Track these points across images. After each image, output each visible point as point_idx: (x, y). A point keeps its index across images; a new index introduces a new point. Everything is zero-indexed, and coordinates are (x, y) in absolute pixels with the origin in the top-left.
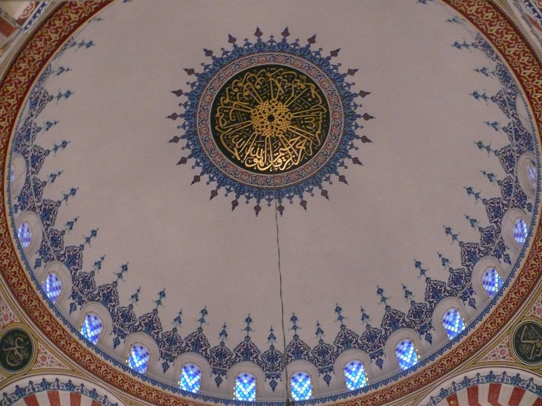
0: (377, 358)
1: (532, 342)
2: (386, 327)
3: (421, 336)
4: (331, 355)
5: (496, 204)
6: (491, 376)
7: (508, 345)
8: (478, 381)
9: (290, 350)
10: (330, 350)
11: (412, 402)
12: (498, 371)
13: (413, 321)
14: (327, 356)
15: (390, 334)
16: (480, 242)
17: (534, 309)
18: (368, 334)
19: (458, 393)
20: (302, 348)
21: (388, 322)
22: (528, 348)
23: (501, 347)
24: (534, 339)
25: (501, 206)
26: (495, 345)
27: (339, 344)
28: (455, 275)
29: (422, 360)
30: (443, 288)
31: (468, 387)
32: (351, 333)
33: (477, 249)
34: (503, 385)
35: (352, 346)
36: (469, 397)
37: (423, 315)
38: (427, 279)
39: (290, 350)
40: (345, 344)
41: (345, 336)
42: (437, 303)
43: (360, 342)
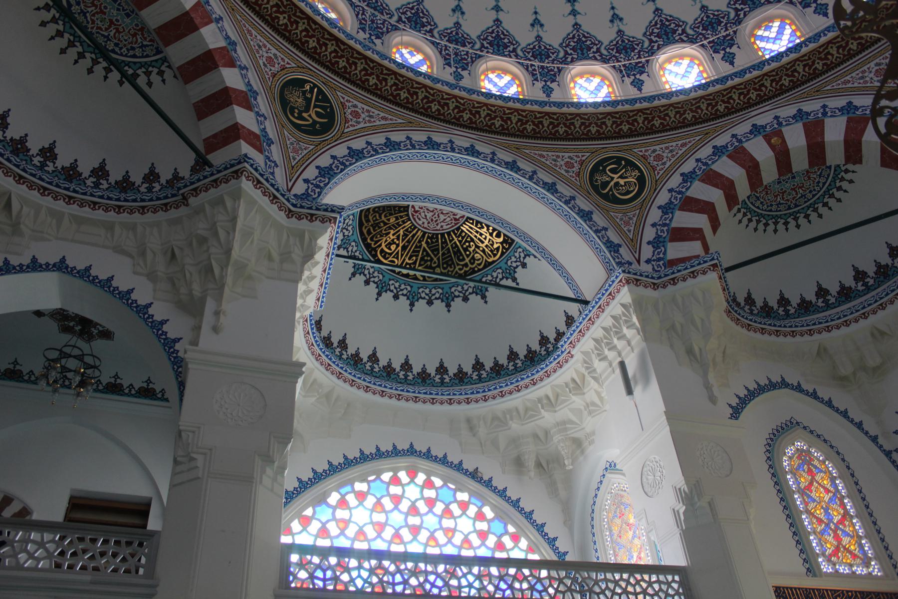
11: (698, 138)
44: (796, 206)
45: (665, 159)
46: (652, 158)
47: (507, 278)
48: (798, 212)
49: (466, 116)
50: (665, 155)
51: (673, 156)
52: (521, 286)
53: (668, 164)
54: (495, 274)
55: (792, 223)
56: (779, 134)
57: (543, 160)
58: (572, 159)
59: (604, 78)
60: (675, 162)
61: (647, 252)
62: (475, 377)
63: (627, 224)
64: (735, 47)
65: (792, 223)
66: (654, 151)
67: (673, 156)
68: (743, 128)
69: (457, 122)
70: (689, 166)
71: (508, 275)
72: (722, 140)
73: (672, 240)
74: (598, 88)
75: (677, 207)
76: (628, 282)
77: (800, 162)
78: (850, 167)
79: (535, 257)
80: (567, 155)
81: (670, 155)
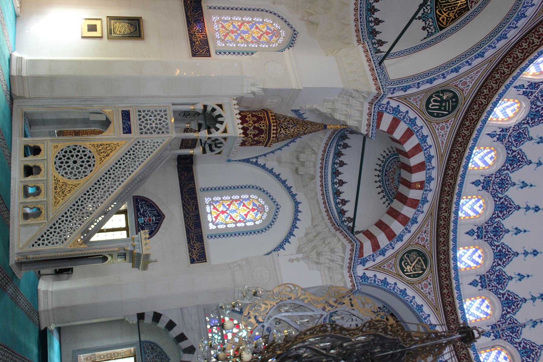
1: (413, 264)
5: (513, 307)
6: (415, 221)
7: (424, 246)
11: (442, 151)
12: (414, 228)
16: (504, 269)
17: (430, 284)
19: (421, 192)
22: (412, 258)
23: (427, 240)
24: (414, 267)
25: (509, 310)
26: (431, 237)
28: (501, 231)
30: (501, 215)
33: (501, 263)
34: (403, 228)
37: (497, 186)
38: (519, 208)
42: (496, 204)
44: (386, 175)
45: (440, 131)
47: (423, 14)
48: (382, 173)
49: (525, 45)
50: (442, 132)
51: (440, 135)
52: (415, 20)
53: (437, 131)
54: (429, 7)
55: (378, 168)
56: (421, 188)
58: (467, 86)
59: (509, 118)
60: (437, 136)
61: (394, 104)
63: (415, 99)
64: (481, 188)
65: (378, 168)
66: (448, 127)
67: (440, 135)
68: (434, 173)
69: (524, 38)
70: (429, 141)
71: (424, 15)
72: (434, 162)
74: (505, 113)
75: (410, 127)
77: (402, 189)
78: (389, 206)
79: (425, 38)
80: (471, 85)
81: (441, 134)
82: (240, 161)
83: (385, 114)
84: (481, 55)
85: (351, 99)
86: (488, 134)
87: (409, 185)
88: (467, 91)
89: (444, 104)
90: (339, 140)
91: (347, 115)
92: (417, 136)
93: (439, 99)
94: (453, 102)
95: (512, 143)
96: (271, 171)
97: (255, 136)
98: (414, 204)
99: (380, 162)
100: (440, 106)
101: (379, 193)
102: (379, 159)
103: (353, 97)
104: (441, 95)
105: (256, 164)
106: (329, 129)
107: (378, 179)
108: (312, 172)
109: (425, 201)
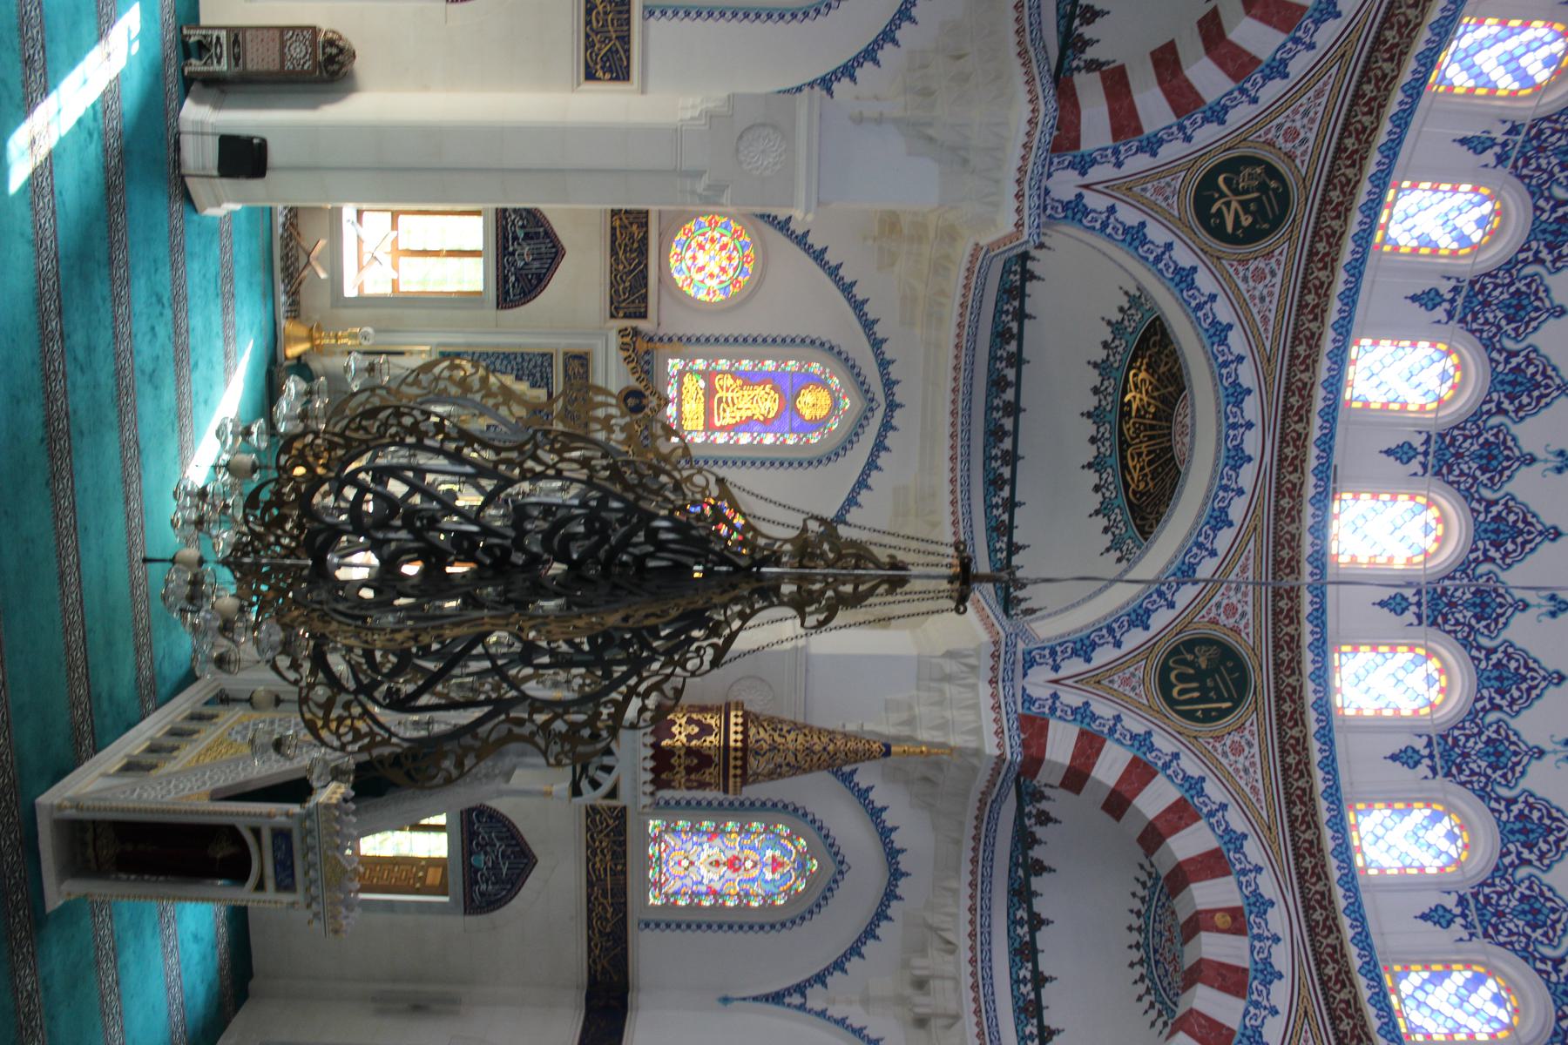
0: (1425, 752)
2: (1521, 806)
3: (1454, 897)
4: (1471, 628)
8: (1257, 1004)
9: (1510, 511)
10: (1487, 627)
11: (1264, 814)
13: (1512, 890)
14: (1469, 614)
15: (1493, 810)
18: (1512, 748)
19: (1242, 943)
20: (1510, 547)
21: (1536, 815)
27: (1500, 655)
29: (1361, 880)
31: (1251, 974)
32: (1530, 695)
35: (1485, 693)
36: (1221, 965)
39: (1510, 511)
40: (1495, 673)
41: (1524, 679)
43: (1493, 717)
44: (1157, 962)
45: (1232, 758)
46: (1237, 739)
50: (1241, 759)
51: (1237, 770)
55: (1136, 955)
57: (1237, 569)
61: (1071, 698)
62: (994, 500)
63: (1125, 682)
65: (1136, 955)
66: (1250, 745)
70: (1214, 791)
73: (1082, 733)
75: (1140, 755)
76: (996, 643)
80: (1249, 609)
82: (755, 999)
83: (1053, 723)
84: (1220, 520)
85: (946, 687)
86: (1394, 757)
87: (1198, 923)
88: (1250, 630)
89: (1209, 683)
90: (1011, 909)
91: (943, 726)
92: (1169, 777)
93: (1191, 671)
94: (1230, 671)
95: (1488, 777)
96: (841, 1022)
97: (690, 737)
98: (1232, 980)
99: (1135, 937)
100: (1203, 689)
101: (1153, 1024)
102: (1130, 928)
103: (948, 678)
104: (1190, 657)
105: (802, 1007)
106: (897, 754)
107: (1141, 988)
108: (952, 1008)
109: (1269, 974)
